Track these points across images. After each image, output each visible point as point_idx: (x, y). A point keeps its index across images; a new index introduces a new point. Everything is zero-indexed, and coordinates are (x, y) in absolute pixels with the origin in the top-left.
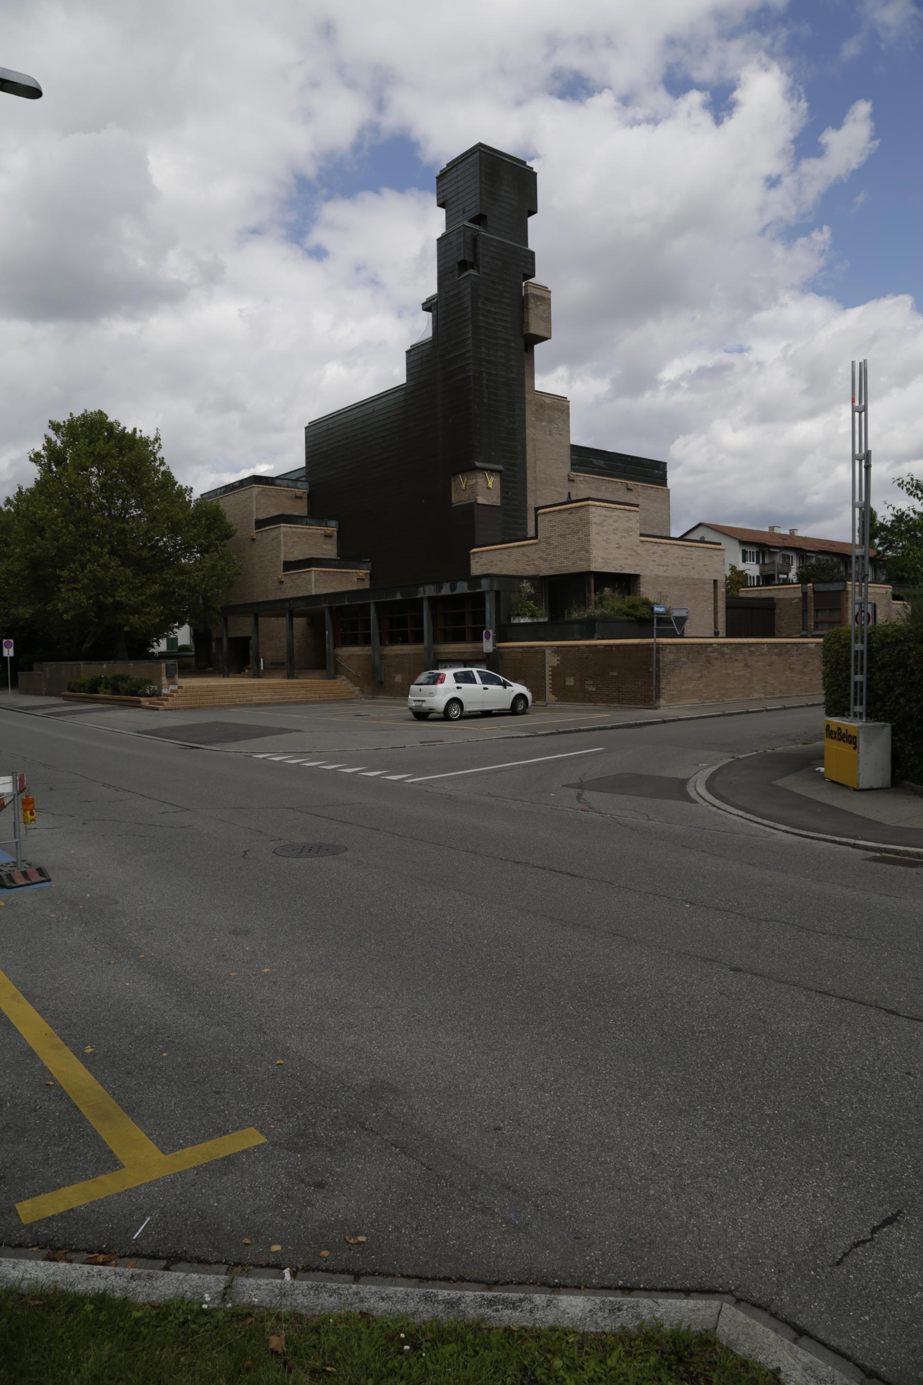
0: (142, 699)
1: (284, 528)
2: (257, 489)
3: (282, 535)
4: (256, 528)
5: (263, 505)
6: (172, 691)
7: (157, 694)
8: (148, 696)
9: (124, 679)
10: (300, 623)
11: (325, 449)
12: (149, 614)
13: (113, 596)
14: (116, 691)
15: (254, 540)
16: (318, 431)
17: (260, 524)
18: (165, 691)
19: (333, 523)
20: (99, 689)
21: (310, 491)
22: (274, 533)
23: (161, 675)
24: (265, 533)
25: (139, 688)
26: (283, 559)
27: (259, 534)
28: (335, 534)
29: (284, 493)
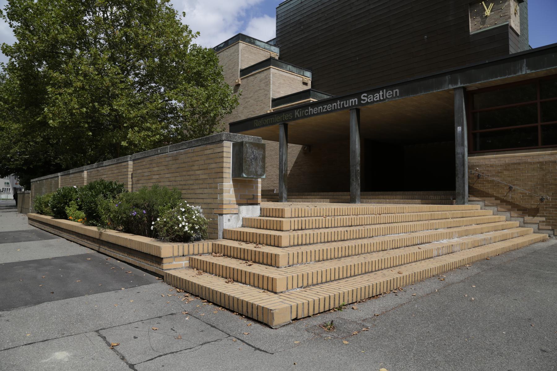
0: (167, 249)
1: (273, 71)
2: (242, 45)
3: (271, 75)
4: (241, 76)
5: (247, 57)
6: (247, 222)
7: (206, 231)
8: (185, 238)
9: (112, 190)
10: (294, 150)
11: (298, 19)
12: (149, 129)
13: (110, 105)
14: (93, 217)
15: (238, 85)
16: (292, 6)
17: (245, 72)
18: (230, 222)
19: (308, 74)
20: (69, 210)
21: (280, 55)
22: (262, 75)
23: (219, 174)
24: (252, 77)
25: (152, 217)
26: (271, 97)
27: (245, 80)
28: (310, 82)
29: (262, 52)
